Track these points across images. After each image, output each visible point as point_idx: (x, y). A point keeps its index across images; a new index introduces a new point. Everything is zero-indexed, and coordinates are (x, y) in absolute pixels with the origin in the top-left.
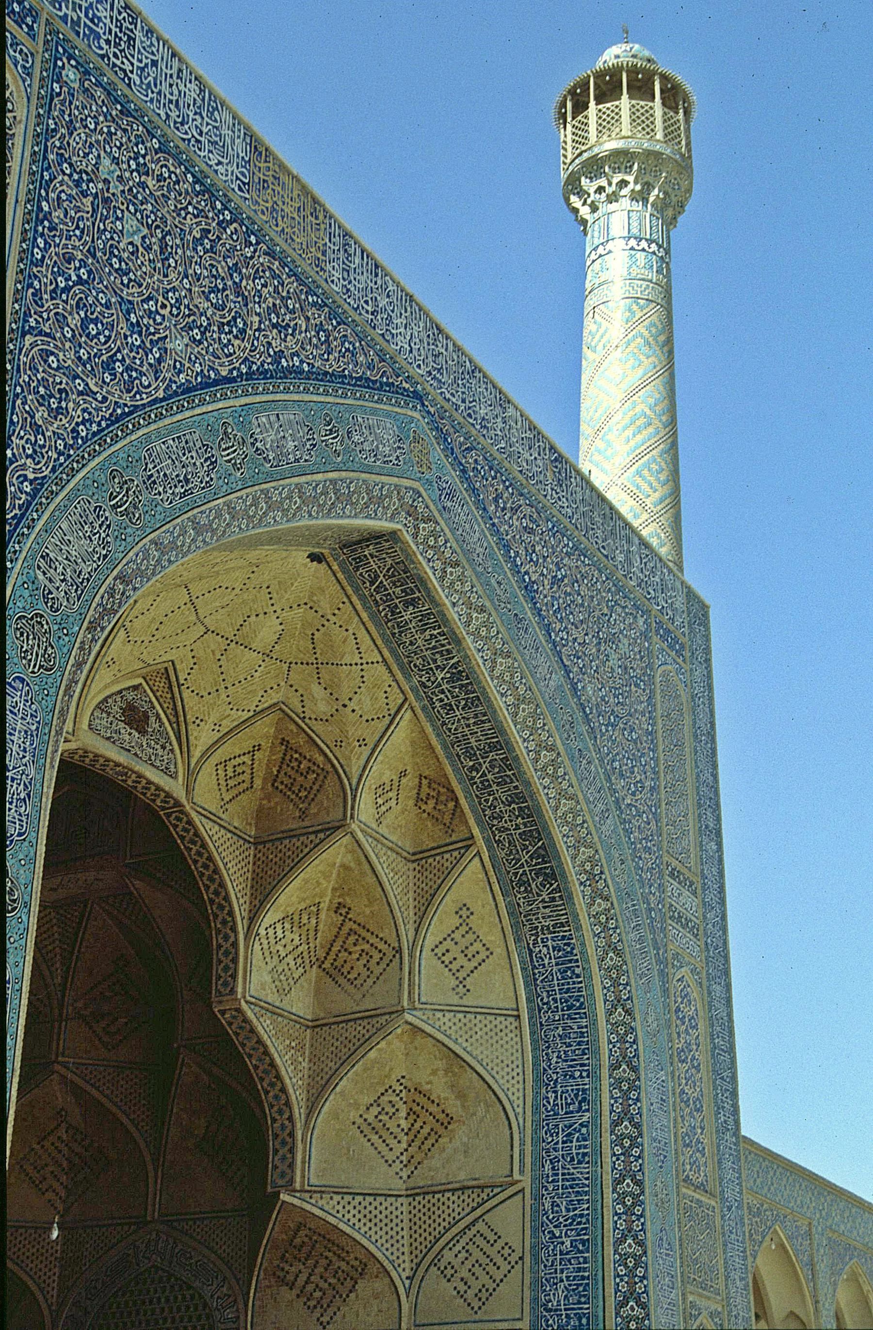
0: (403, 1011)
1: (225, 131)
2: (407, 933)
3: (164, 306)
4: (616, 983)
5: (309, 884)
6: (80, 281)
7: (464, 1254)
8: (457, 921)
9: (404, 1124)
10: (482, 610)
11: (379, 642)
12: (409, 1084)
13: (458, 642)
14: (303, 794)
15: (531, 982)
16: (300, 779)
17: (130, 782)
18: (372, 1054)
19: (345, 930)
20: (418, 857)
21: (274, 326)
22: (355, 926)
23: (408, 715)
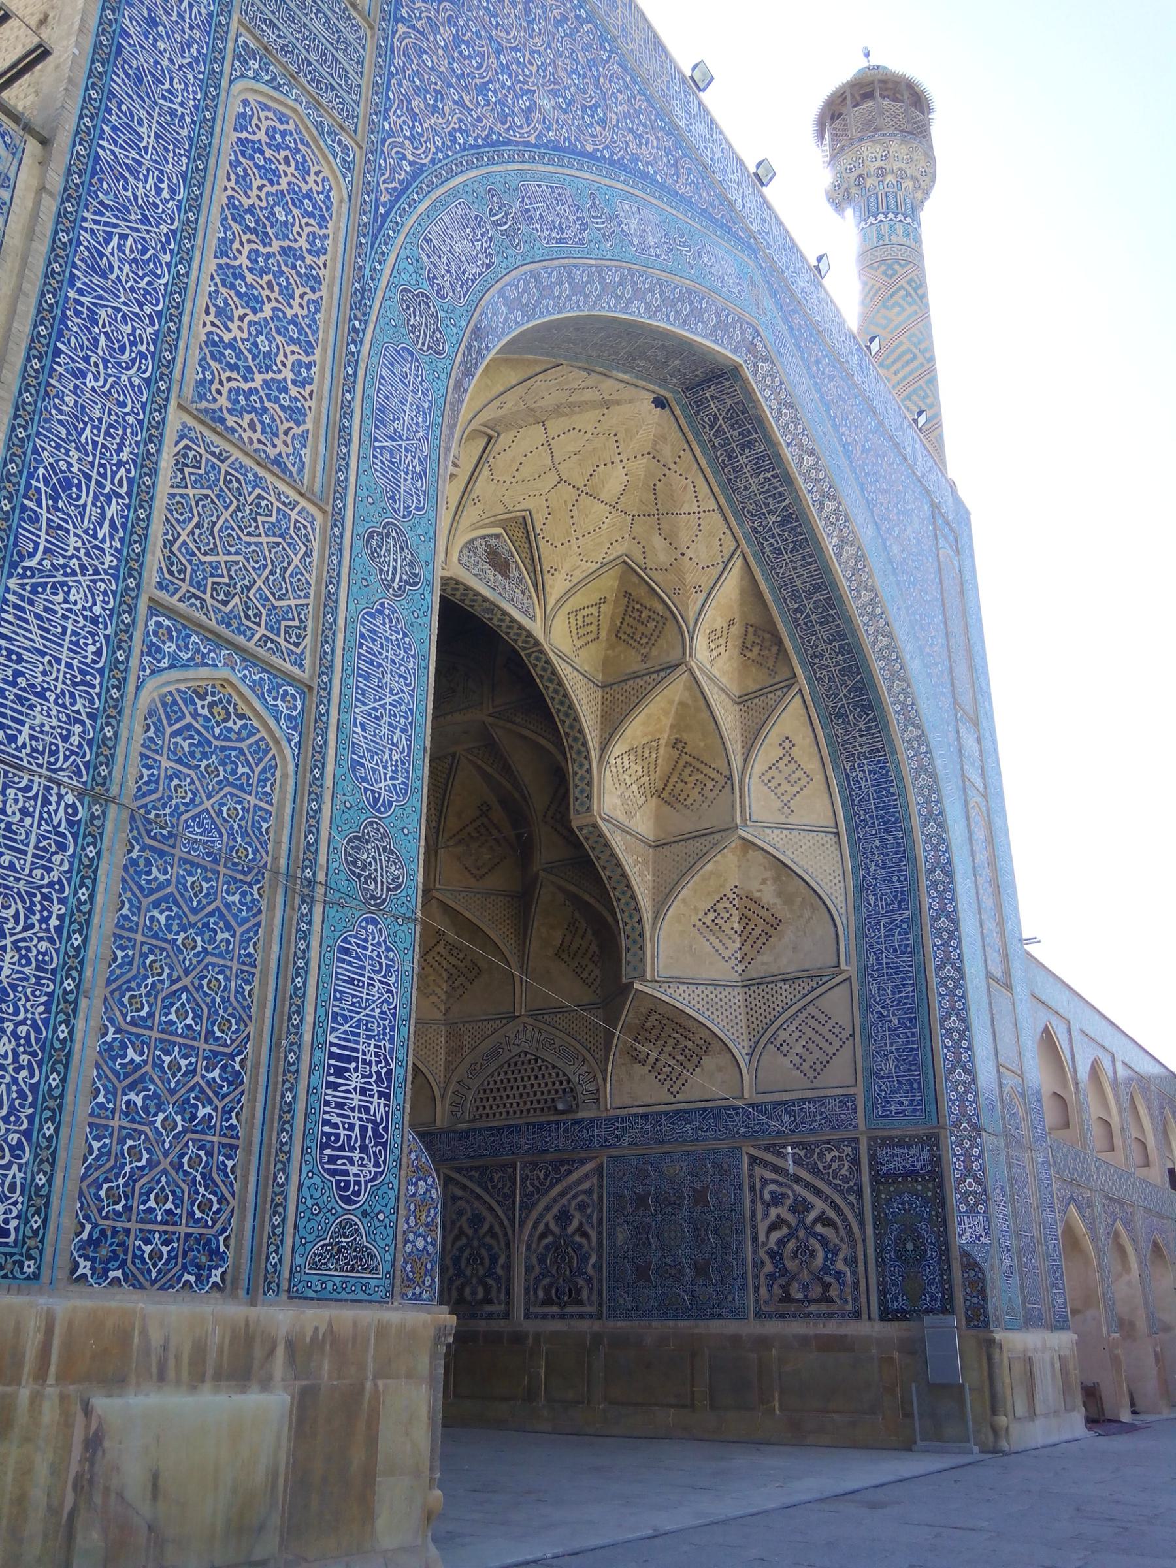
2: (737, 762)
4: (928, 801)
5: (650, 721)
7: (797, 1034)
8: (780, 752)
11: (716, 489)
12: (743, 894)
14: (644, 641)
15: (849, 803)
16: (641, 628)
17: (495, 621)
18: (709, 867)
19: (681, 763)
20: (744, 700)
22: (690, 760)
23: (738, 562)
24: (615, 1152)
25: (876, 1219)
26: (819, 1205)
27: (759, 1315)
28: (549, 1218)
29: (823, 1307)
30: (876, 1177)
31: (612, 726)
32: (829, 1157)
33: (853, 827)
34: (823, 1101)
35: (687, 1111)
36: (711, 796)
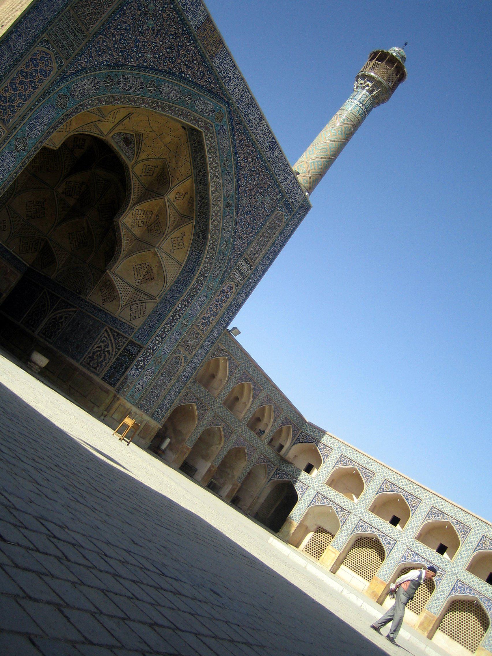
0: (155, 247)
1: (199, 12)
3: (149, 45)
4: (205, 271)
6: (125, 29)
8: (181, 236)
9: (144, 273)
10: (217, 163)
13: (206, 167)
15: (188, 259)
19: (156, 222)
21: (186, 65)
23: (191, 179)
24: (81, 309)
25: (118, 358)
26: (110, 348)
27: (81, 364)
28: (58, 315)
29: (94, 370)
30: (124, 349)
31: (140, 200)
32: (120, 339)
33: (185, 266)
34: (128, 326)
35: (102, 310)
36: (157, 235)
